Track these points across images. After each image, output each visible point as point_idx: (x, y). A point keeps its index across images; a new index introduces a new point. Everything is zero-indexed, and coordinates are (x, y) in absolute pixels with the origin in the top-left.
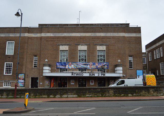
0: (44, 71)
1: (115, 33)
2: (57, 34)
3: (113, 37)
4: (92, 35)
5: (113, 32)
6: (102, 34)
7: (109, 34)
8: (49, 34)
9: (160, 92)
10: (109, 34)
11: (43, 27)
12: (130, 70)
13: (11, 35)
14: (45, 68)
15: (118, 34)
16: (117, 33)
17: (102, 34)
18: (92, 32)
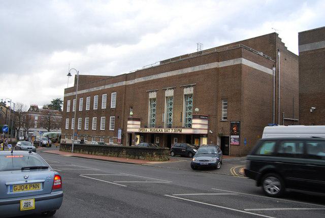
0: (128, 126)
1: (204, 65)
2: (147, 77)
3: (203, 72)
4: (179, 73)
5: (203, 64)
6: (189, 70)
7: (197, 68)
8: (141, 78)
9: (161, 157)
10: (197, 68)
11: (168, 65)
12: (222, 123)
13: (115, 85)
14: (129, 122)
15: (208, 65)
16: (207, 65)
17: (189, 70)
18: (180, 68)
